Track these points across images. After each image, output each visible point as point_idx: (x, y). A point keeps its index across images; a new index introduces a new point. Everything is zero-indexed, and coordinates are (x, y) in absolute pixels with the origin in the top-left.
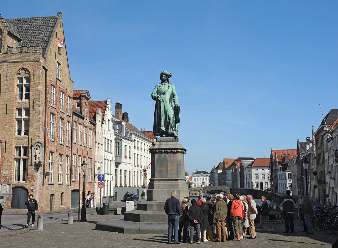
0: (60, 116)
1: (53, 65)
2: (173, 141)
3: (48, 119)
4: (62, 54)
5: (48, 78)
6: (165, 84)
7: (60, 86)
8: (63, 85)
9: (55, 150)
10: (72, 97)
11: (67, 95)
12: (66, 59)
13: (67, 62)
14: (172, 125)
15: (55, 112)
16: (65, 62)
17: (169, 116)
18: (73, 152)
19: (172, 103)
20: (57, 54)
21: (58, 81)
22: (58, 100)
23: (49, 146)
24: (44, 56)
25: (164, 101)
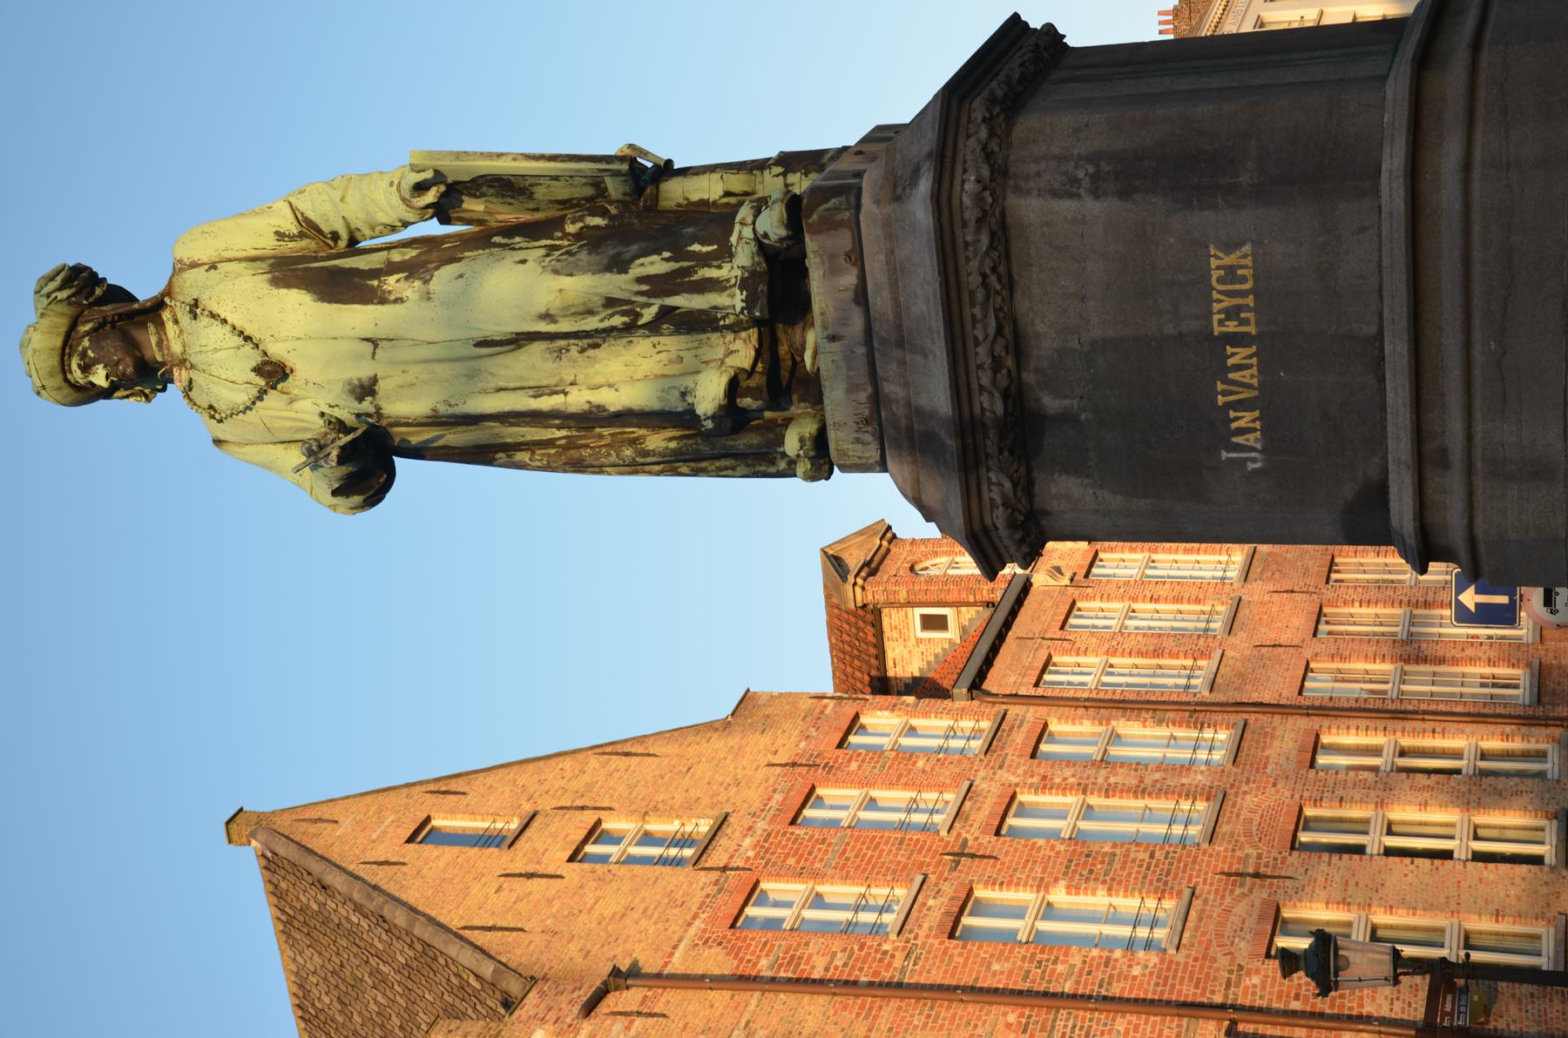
0: (984, 833)
1: (590, 902)
2: (856, 256)
3: (1000, 973)
4: (528, 808)
5: (677, 965)
6: (176, 348)
7: (761, 825)
8: (754, 797)
9: (1261, 894)
10: (849, 709)
11: (831, 753)
12: (567, 763)
13: (594, 762)
14: (656, 265)
15: (948, 889)
16: (586, 778)
17: (547, 316)
18: (1288, 694)
19: (392, 268)
20: (518, 860)
21: (717, 857)
22: (863, 852)
23: (1223, 961)
24: (515, 987)
25: (364, 372)
